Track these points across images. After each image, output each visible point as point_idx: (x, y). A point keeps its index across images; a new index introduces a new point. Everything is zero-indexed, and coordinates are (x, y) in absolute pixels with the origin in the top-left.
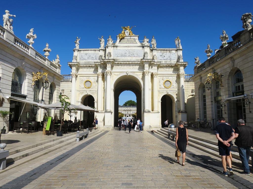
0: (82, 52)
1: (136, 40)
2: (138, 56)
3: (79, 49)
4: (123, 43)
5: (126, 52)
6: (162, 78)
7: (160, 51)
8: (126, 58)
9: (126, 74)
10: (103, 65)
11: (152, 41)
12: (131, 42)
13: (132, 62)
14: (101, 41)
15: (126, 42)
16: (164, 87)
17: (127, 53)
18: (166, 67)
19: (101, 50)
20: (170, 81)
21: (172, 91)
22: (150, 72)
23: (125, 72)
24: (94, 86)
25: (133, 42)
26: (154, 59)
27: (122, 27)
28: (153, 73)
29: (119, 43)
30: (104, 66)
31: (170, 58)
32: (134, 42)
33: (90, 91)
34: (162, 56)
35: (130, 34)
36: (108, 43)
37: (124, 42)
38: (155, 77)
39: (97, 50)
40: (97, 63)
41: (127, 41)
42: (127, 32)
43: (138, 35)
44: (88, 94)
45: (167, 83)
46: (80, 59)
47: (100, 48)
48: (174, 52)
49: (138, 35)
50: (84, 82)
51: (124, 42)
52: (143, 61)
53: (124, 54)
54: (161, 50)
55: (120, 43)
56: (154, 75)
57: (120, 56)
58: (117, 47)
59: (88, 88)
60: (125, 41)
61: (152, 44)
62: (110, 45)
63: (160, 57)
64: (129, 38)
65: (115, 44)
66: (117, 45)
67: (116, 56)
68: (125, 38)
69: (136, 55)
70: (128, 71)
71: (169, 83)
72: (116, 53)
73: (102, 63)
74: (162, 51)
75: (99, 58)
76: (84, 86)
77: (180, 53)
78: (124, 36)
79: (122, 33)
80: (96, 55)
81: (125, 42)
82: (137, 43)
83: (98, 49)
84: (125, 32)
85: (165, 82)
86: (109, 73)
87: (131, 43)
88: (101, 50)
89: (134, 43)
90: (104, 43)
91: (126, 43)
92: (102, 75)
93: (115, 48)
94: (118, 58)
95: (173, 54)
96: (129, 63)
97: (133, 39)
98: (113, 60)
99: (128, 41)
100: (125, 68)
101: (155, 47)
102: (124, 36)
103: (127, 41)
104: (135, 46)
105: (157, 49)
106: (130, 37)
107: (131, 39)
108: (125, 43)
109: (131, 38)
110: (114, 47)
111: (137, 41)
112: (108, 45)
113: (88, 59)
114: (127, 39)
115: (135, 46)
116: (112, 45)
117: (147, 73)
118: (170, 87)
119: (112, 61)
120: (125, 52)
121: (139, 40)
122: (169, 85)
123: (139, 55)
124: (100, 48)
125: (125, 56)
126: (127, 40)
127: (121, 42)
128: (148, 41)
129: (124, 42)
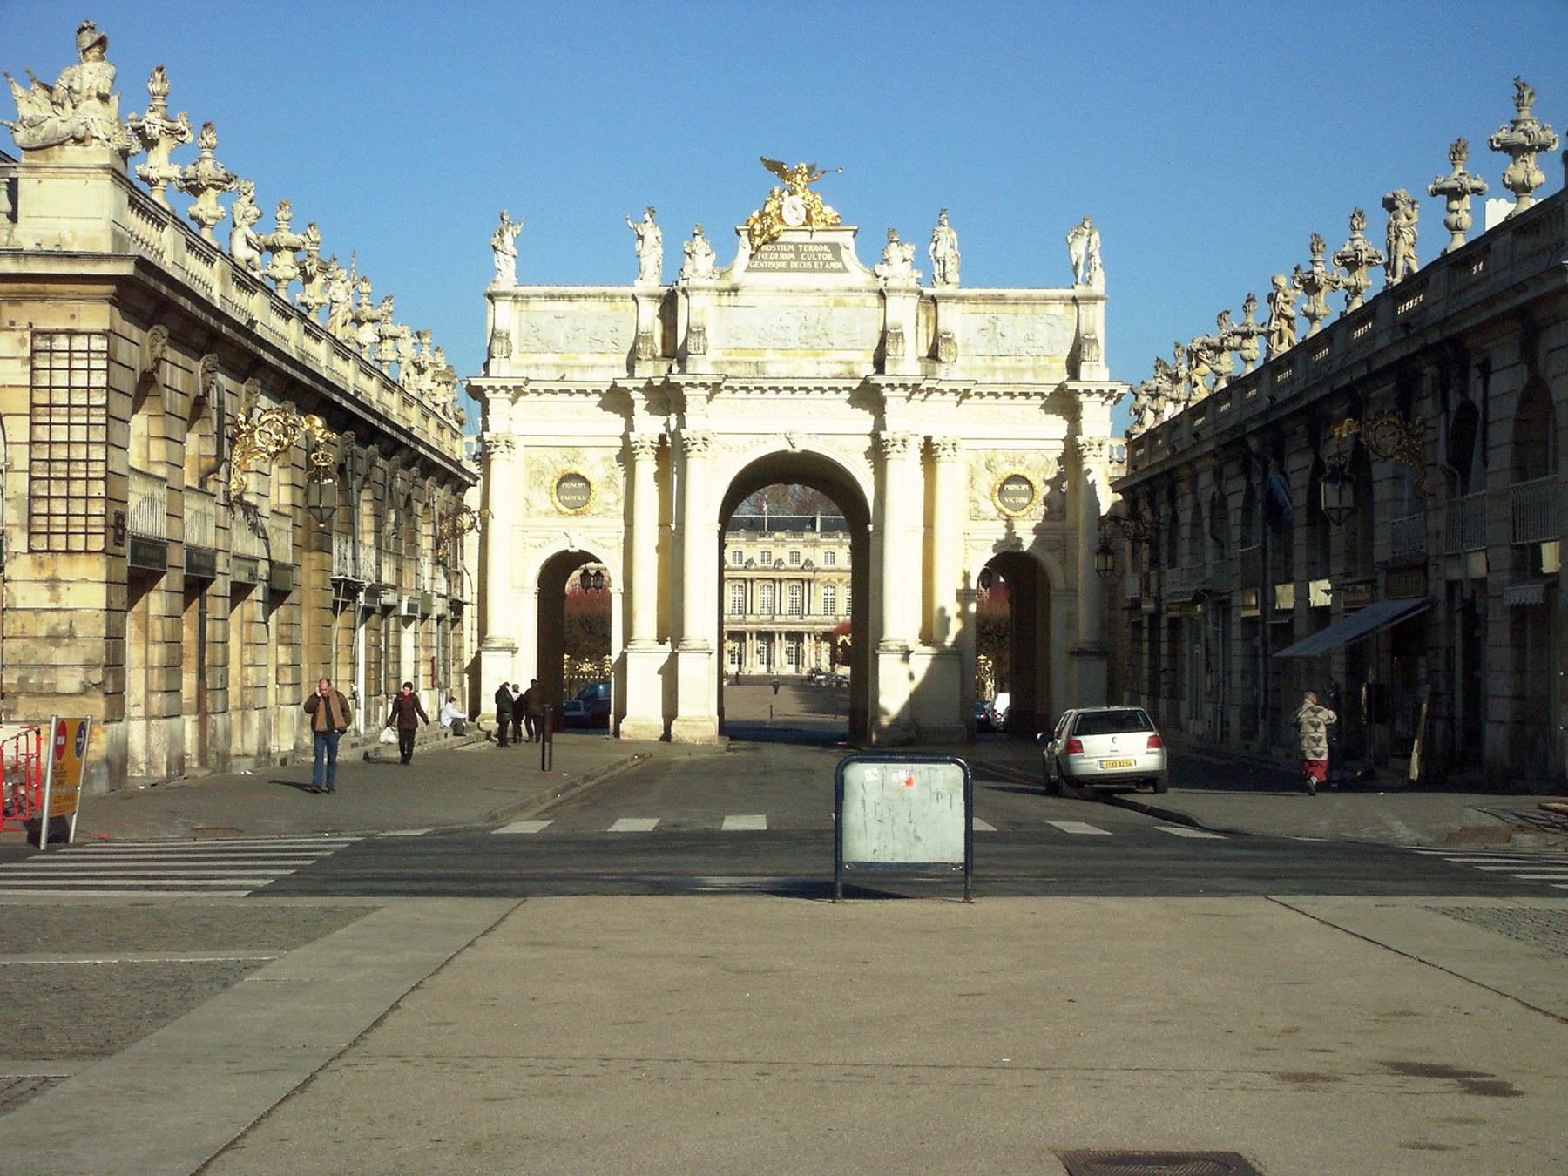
0: (535, 305)
1: (843, 252)
4: (774, 270)
6: (983, 462)
9: (782, 446)
12: (813, 262)
15: (788, 262)
24: (607, 504)
25: (825, 262)
28: (934, 441)
29: (748, 269)
35: (808, 217)
37: (774, 260)
41: (793, 256)
45: (1011, 487)
47: (639, 287)
48: (1058, 309)
50: (551, 479)
51: (774, 260)
55: (755, 270)
56: (940, 452)
59: (577, 514)
71: (1025, 487)
77: (1095, 319)
81: (784, 264)
84: (780, 207)
85: (1002, 486)
89: (832, 270)
91: (789, 270)
95: (1054, 321)
97: (825, 248)
99: (798, 259)
103: (793, 256)
107: (816, 248)
108: (780, 270)
111: (849, 257)
114: (792, 247)
120: (784, 324)
122: (1025, 500)
126: (791, 252)
127: (762, 260)
129: (779, 264)
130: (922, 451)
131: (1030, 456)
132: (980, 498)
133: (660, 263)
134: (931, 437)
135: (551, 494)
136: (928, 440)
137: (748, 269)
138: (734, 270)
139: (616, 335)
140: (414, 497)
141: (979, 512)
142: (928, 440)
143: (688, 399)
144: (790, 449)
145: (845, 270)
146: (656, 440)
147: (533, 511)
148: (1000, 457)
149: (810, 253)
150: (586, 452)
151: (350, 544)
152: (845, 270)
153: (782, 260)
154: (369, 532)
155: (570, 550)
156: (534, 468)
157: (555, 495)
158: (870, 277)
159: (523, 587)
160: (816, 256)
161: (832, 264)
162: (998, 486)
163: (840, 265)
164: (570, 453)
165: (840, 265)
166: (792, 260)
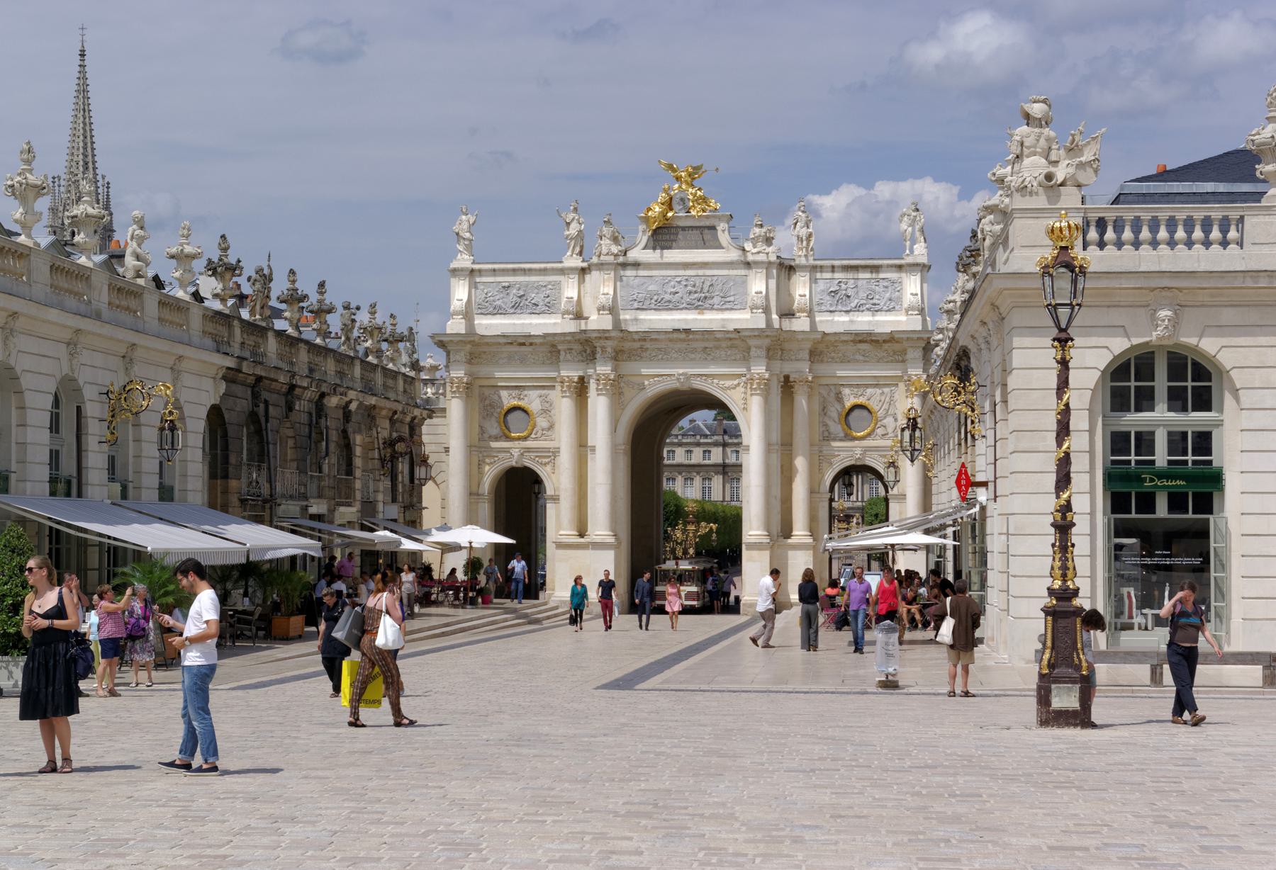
2: (727, 306)
3: (476, 267)
6: (832, 395)
16: (842, 435)
18: (852, 344)
19: (572, 270)
20: (869, 407)
21: (876, 449)
28: (791, 379)
31: (874, 301)
33: (528, 450)
44: (519, 465)
45: (856, 413)
46: (480, 311)
52: (745, 336)
53: (667, 297)
56: (796, 387)
57: (653, 306)
58: (636, 265)
59: (519, 439)
63: (828, 298)
67: (636, 305)
71: (865, 413)
74: (837, 275)
76: (498, 429)
82: (723, 248)
93: (630, 273)
98: (621, 335)
113: (512, 311)
118: (869, 435)
120: (673, 290)
123: (732, 299)
130: (782, 387)
131: (869, 391)
132: (830, 423)
135: (499, 422)
136: (787, 378)
139: (547, 300)
140: (350, 430)
141: (829, 433)
142: (787, 378)
146: (576, 379)
147: (486, 436)
148: (846, 391)
150: (526, 392)
151: (264, 473)
154: (292, 460)
155: (514, 464)
156: (487, 402)
157: (503, 425)
158: (740, 252)
159: (478, 495)
161: (711, 243)
162: (844, 414)
164: (514, 393)
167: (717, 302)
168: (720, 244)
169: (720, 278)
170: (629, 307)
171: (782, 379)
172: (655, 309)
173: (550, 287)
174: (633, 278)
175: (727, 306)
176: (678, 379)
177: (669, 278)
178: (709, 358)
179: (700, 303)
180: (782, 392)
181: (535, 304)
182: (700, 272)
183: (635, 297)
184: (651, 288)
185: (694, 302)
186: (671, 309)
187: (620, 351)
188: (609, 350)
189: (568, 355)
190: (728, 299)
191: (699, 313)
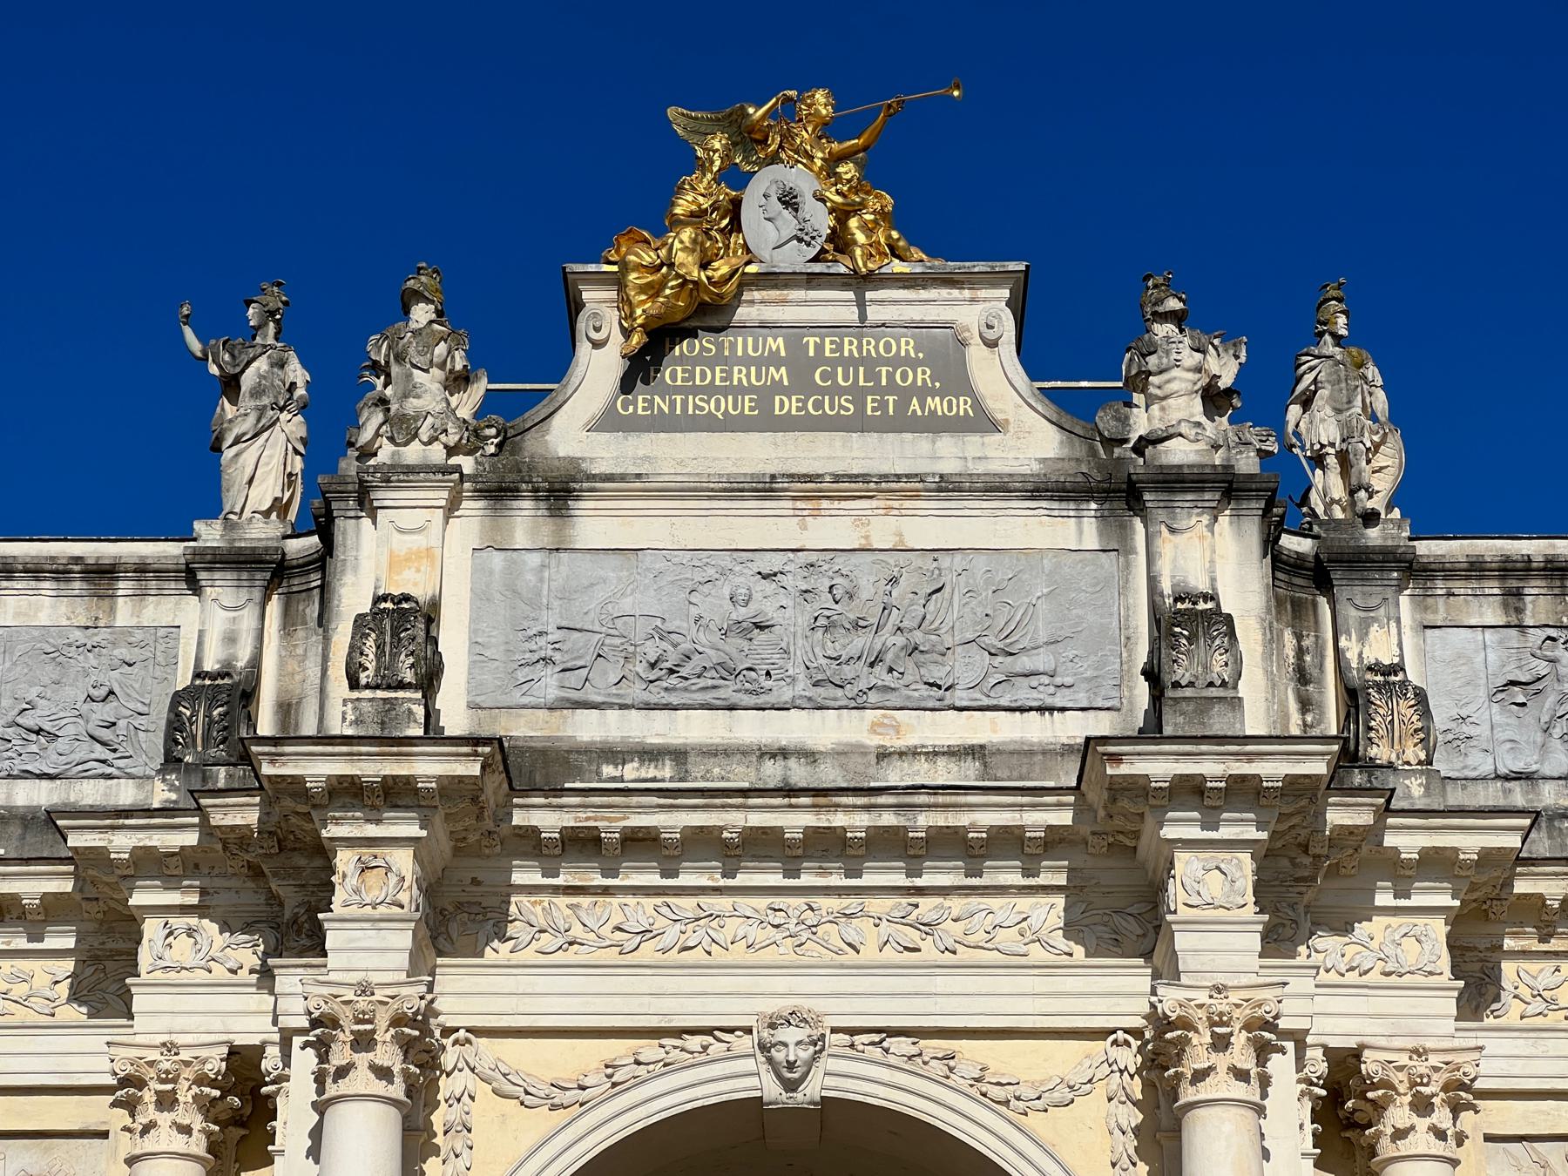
1: (976, 353)
2: (1023, 693)
5: (767, 600)
7: (1493, 587)
8: (750, 728)
10: (256, 873)
11: (1307, 402)
12: (859, 395)
13: (888, 819)
14: (230, 386)
15: (765, 395)
17: (790, 617)
22: (1299, 1039)
23: (745, 1043)
25: (905, 395)
26: (1380, 752)
27: (672, 112)
28: (1371, 1064)
29: (608, 422)
30: (274, 899)
32: (923, 393)
34: (1551, 700)
35: (840, 241)
36: (372, 422)
37: (710, 390)
38: (1421, 1141)
39: (142, 569)
40: (122, 843)
42: (789, 200)
43: (1021, 266)
49: (1021, 266)
51: (710, 390)
52: (1139, 788)
54: (1513, 572)
56: (1399, 1114)
57: (636, 692)
60: (739, 374)
61: (1318, 461)
62: (413, 453)
64: (835, 306)
65: (531, 444)
66: (573, 461)
67: (550, 685)
68: (743, 313)
69: (966, 669)
70: (805, 1004)
72: (550, 621)
73: (235, 839)
75: (175, 725)
78: (721, 268)
79: (677, 223)
80: (113, 679)
83: (170, 551)
84: (736, 204)
86: (387, 1054)
87: (859, 424)
88: (239, 561)
89: (935, 425)
90: (293, 426)
91: (767, 422)
92: (207, 1108)
94: (588, 728)
96: (812, 834)
98: (474, 769)
99: (801, 384)
100: (738, 953)
101: (1371, 518)
102: (721, 268)
104: (948, 486)
105: (1425, 548)
106: (861, 304)
109: (875, 314)
110: (498, 492)
112: (386, 452)
114: (777, 344)
115: (948, 486)
116: (467, 464)
117: (1241, 1053)
119: (450, 788)
120: (741, 613)
121: (1033, 373)
123: (1041, 661)
124: (209, 534)
125: (728, 692)
126: (774, 360)
127: (666, 391)
128: (1226, 370)
129: (727, 404)
133: (298, 464)
134: (1356, 1054)
137: (608, 422)
138: (558, 421)
139: (106, 712)
142: (1345, 1063)
143: (345, 860)
144: (772, 1090)
145: (984, 422)
146: (215, 1063)
149: (849, 363)
152: (984, 422)
153: (740, 390)
160: (872, 375)
161: (933, 403)
163: (963, 406)
165: (963, 406)
166: (777, 387)
167: (966, 677)
168: (977, 404)
169: (981, 562)
170: (517, 697)
171: (1323, 1068)
172: (648, 707)
173: (122, 652)
174: (535, 559)
175: (1023, 693)
176: (764, 1047)
177: (726, 560)
178: (929, 951)
179: (880, 675)
180: (1318, 1140)
181: (38, 732)
182: (883, 532)
183: (543, 646)
184: (626, 605)
185: (848, 671)
186: (732, 708)
187: (459, 906)
188: (403, 860)
189: (181, 944)
190: (1024, 663)
191: (874, 728)
